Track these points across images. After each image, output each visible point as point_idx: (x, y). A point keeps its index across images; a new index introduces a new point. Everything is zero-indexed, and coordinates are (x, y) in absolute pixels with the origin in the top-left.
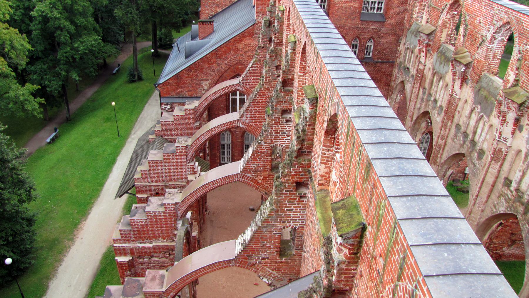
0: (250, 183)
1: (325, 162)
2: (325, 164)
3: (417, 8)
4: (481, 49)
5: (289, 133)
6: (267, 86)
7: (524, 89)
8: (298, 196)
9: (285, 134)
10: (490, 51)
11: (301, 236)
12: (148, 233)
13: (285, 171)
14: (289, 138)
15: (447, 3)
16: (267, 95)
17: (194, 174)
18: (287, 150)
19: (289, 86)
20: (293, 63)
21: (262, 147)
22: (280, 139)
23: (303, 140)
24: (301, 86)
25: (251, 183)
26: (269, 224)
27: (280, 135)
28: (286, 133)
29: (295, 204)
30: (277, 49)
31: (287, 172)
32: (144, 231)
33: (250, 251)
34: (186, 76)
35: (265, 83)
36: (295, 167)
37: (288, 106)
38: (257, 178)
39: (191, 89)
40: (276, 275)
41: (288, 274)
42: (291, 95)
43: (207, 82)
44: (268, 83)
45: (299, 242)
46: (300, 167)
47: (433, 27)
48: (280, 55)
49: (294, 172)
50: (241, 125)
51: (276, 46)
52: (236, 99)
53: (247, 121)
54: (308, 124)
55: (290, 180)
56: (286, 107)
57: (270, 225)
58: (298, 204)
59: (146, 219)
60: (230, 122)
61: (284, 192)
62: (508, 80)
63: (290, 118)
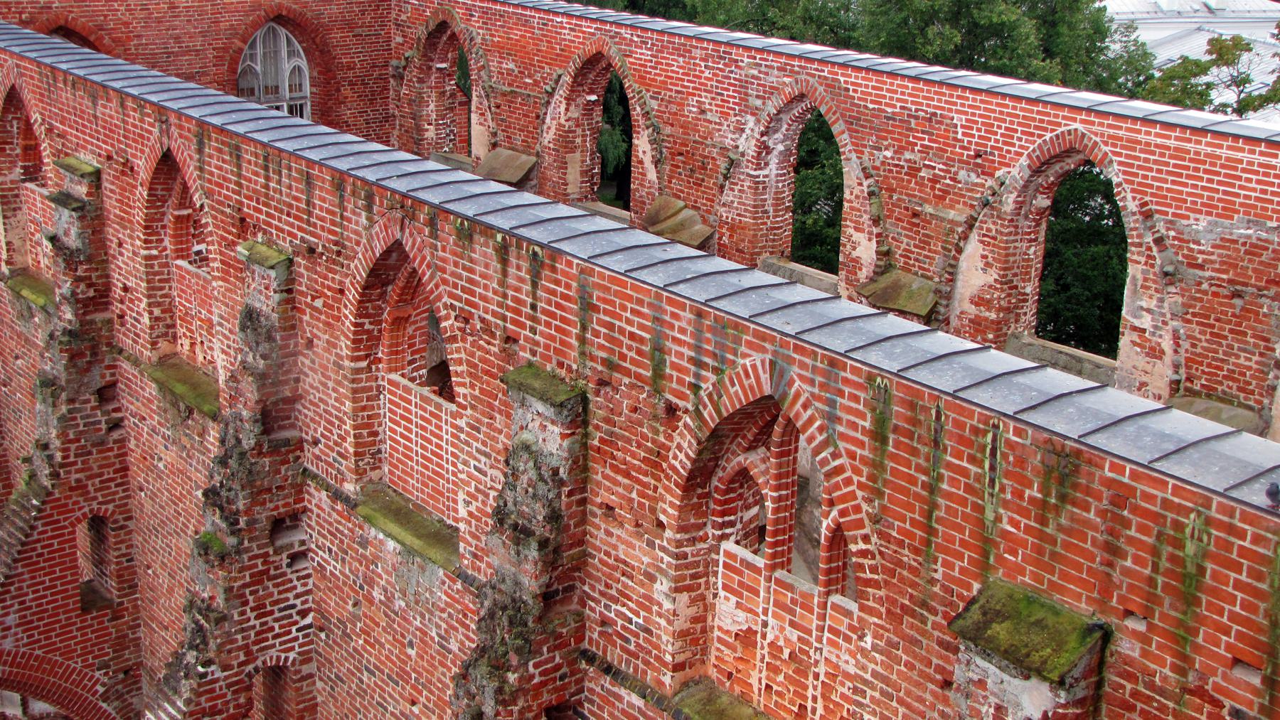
1: (688, 582)
2: (689, 589)
3: (432, 106)
4: (732, 190)
5: (306, 602)
6: (75, 476)
7: (916, 274)
9: (293, 611)
10: (764, 188)
13: (504, 681)
14: (308, 620)
15: (560, 72)
16: (79, 514)
18: (306, 669)
19: (282, 428)
20: (290, 337)
21: (213, 690)
22: (275, 637)
23: (557, 551)
24: (364, 408)
27: (276, 620)
30: (92, 322)
31: (520, 679)
35: (62, 466)
36: (542, 654)
37: (291, 500)
42: (299, 457)
44: (75, 463)
46: (556, 648)
47: (524, 157)
48: (109, 344)
49: (541, 674)
51: (85, 314)
54: (566, 489)
56: (284, 506)
62: (856, 260)
63: (303, 543)
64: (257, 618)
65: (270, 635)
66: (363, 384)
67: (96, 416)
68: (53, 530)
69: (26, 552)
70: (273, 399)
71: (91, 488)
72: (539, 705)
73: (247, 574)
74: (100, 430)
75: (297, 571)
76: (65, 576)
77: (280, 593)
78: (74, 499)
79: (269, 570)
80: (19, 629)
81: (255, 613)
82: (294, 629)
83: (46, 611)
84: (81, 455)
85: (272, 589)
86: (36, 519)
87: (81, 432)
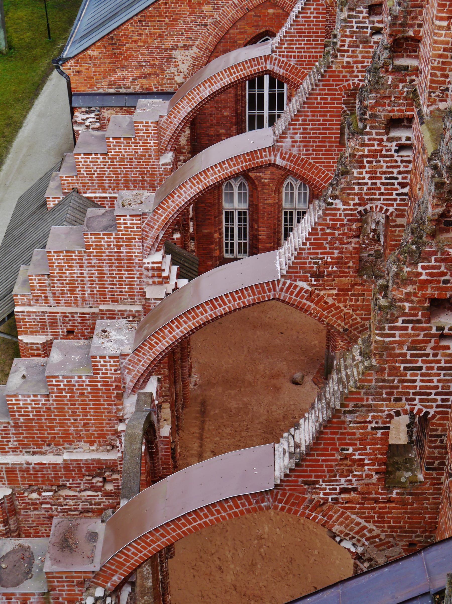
0: (305, 304)
6: (346, 59)
8: (433, 335)
9: (396, 182)
11: (440, 436)
12: (52, 428)
13: (402, 270)
14: (406, 190)
17: (160, 283)
18: (399, 221)
22: (381, 194)
25: (308, 303)
26: (359, 403)
28: (396, 178)
29: (427, 355)
32: (40, 425)
33: (311, 471)
34: (135, 37)
35: (339, 51)
36: (430, 262)
38: (322, 293)
39: (147, 70)
40: (377, 531)
41: (406, 532)
43: (187, 52)
44: (348, 51)
45: (436, 451)
46: (442, 260)
50: (279, 161)
52: (261, 96)
53: (295, 151)
55: (415, 295)
56: (398, 111)
57: (363, 406)
58: (435, 355)
59: (48, 396)
60: (252, 154)
61: (399, 323)
64: (369, 178)
65: (377, 192)
66: (442, 38)
67: (365, 23)
68: (329, 90)
69: (311, 99)
70: (400, 35)
71: (355, 69)
72: (423, 295)
73: (366, 149)
74: (367, 33)
75: (402, 156)
76: (333, 120)
77: (387, 167)
78: (344, 74)
79: (382, 150)
80: (302, 144)
81: (369, 175)
82: (395, 193)
83: (319, 138)
84: (352, 47)
85: (382, 163)
86: (319, 80)
87: (354, 32)
